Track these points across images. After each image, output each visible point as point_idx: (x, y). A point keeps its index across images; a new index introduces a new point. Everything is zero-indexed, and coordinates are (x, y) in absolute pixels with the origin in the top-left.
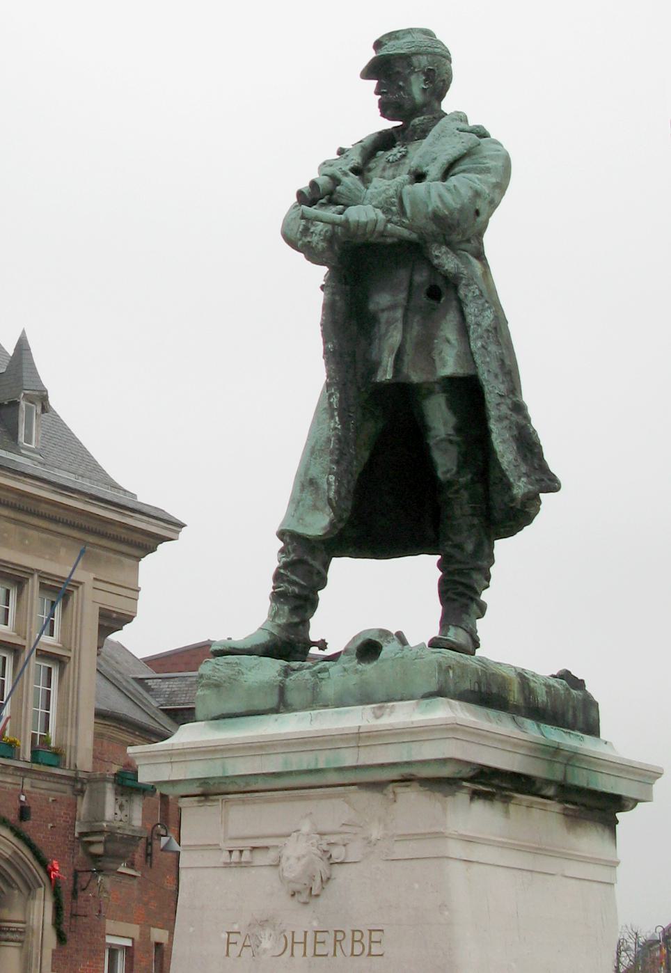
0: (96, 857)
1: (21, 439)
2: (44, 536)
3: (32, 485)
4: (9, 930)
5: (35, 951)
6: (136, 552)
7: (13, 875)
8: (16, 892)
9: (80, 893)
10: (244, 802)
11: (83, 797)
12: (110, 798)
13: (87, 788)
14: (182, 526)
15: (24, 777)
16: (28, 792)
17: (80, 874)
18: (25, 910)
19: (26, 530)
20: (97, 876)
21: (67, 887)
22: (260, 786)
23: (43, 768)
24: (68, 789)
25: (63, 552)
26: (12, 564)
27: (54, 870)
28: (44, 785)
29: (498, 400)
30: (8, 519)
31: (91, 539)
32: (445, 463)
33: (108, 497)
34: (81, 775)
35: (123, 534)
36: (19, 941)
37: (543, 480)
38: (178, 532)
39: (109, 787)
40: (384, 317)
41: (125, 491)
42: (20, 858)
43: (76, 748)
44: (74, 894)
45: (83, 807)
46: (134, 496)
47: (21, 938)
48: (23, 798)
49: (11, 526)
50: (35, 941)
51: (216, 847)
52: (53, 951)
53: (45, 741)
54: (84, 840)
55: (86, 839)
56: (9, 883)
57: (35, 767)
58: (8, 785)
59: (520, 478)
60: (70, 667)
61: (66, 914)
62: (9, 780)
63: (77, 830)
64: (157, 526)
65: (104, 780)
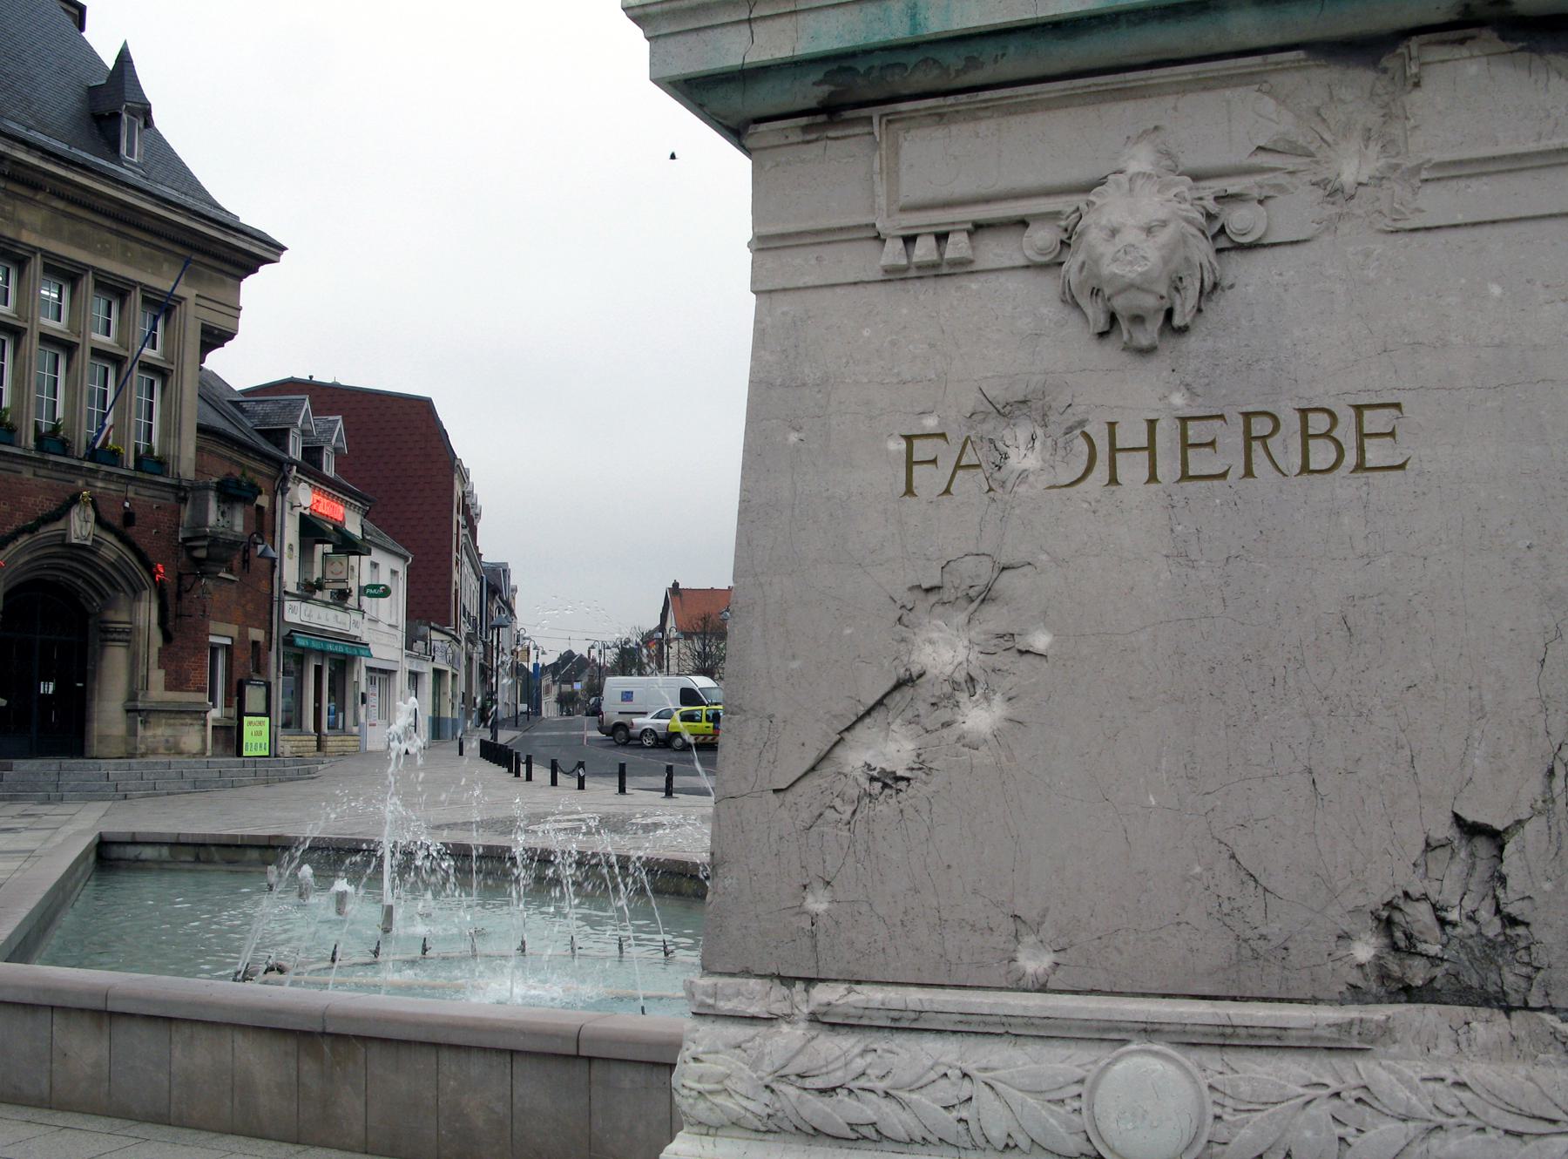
0: (198, 562)
1: (123, 151)
2: (145, 249)
3: (136, 197)
4: (116, 631)
5: (142, 650)
7: (119, 579)
8: (122, 594)
9: (184, 595)
11: (186, 504)
12: (213, 506)
13: (190, 495)
14: (283, 249)
16: (132, 499)
18: (131, 612)
19: (125, 241)
20: (200, 580)
21: (171, 589)
23: (147, 476)
24: (172, 497)
25: (166, 267)
26: (114, 275)
27: (160, 573)
30: (110, 230)
31: (195, 257)
36: (126, 641)
38: (279, 255)
42: (126, 562)
43: (179, 457)
44: (179, 596)
45: (186, 513)
47: (128, 638)
48: (127, 504)
49: (114, 238)
50: (142, 641)
52: (159, 649)
53: (150, 449)
54: (187, 546)
55: (188, 544)
56: (114, 585)
57: (139, 474)
58: (112, 492)
60: (172, 380)
61: (171, 614)
62: (113, 487)
63: (181, 536)
65: (207, 487)
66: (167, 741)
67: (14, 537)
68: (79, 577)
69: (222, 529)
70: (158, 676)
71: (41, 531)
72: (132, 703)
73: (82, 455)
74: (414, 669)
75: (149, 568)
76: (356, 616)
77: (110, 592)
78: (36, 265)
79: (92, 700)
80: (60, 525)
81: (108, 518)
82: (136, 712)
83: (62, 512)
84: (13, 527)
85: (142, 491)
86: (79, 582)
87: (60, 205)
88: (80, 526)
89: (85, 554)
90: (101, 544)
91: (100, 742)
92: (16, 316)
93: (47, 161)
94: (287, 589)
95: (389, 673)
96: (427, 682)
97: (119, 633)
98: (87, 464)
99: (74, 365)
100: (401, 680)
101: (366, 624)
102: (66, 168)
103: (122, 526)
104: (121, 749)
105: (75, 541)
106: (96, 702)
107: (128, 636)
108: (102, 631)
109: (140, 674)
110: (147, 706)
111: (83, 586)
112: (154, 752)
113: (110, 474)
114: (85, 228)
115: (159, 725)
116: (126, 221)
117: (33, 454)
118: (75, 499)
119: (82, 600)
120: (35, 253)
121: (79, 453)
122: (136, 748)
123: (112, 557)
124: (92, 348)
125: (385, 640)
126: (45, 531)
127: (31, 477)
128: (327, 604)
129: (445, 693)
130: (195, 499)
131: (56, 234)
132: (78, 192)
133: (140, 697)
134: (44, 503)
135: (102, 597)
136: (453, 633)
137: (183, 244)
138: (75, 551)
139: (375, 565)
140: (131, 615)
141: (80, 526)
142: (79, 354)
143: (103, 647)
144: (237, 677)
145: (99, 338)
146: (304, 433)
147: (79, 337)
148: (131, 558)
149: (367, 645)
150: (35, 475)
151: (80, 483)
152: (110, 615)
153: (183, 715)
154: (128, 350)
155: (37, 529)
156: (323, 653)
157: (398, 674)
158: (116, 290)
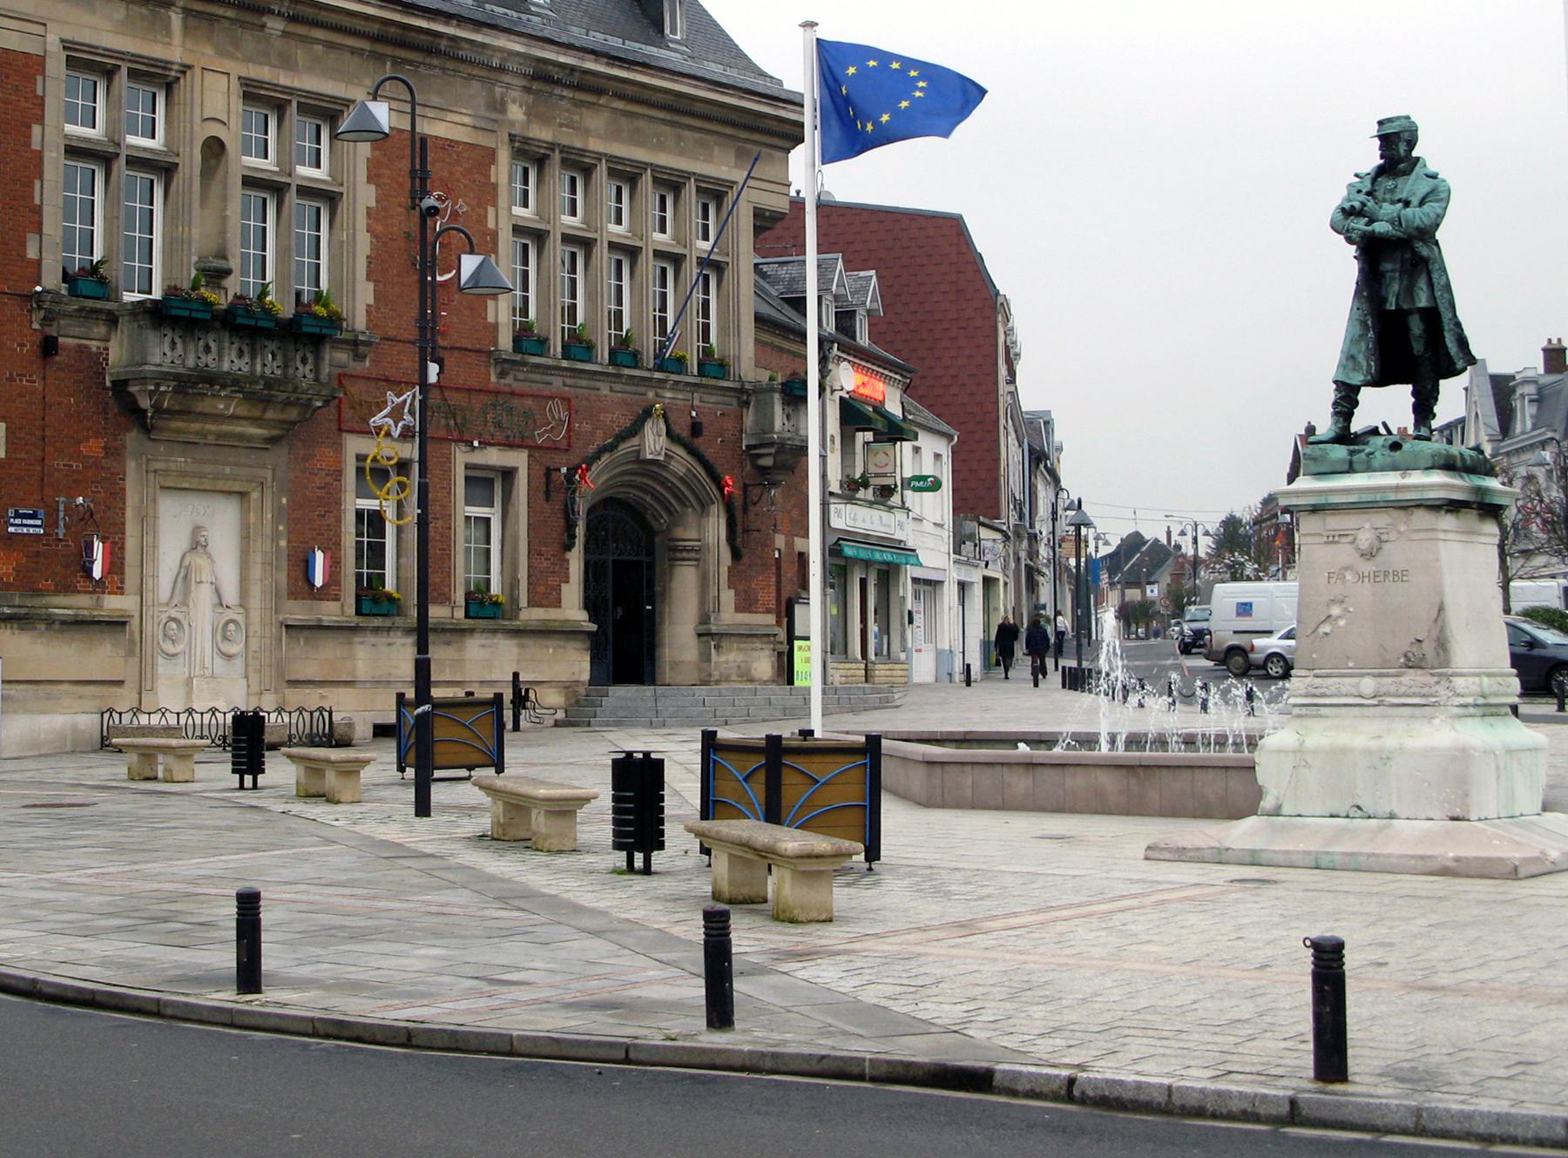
0: (763, 471)
1: (667, 31)
2: (697, 135)
4: (685, 549)
5: (712, 569)
6: (786, 144)
7: (688, 493)
9: (751, 508)
12: (778, 408)
13: (753, 399)
18: (700, 527)
21: (738, 503)
24: (735, 402)
28: (713, 399)
30: (664, 122)
31: (743, 135)
33: (760, 90)
34: (747, 386)
35: (774, 125)
36: (696, 560)
39: (777, 396)
41: (771, 77)
44: (745, 510)
45: (749, 418)
46: (780, 83)
48: (694, 414)
49: (667, 129)
50: (712, 558)
53: (707, 352)
54: (752, 453)
56: (681, 499)
57: (704, 381)
60: (728, 274)
61: (739, 529)
62: (680, 396)
63: (744, 443)
65: (772, 390)
66: (739, 667)
68: (647, 492)
69: (789, 435)
70: (728, 597)
73: (651, 365)
74: (963, 578)
76: (900, 516)
77: (678, 508)
78: (602, 170)
79: (662, 622)
80: (635, 441)
81: (676, 429)
82: (708, 636)
83: (635, 429)
85: (707, 398)
86: (648, 498)
87: (619, 105)
88: (653, 442)
90: (672, 458)
91: (672, 669)
92: (584, 226)
93: (612, 65)
94: (831, 489)
95: (934, 584)
96: (978, 590)
98: (657, 375)
99: (638, 272)
100: (950, 593)
101: (910, 525)
102: (628, 69)
103: (689, 436)
104: (694, 676)
107: (697, 554)
109: (711, 595)
110: (722, 629)
112: (727, 680)
113: (677, 383)
114: (641, 123)
115: (731, 650)
116: (680, 109)
117: (611, 370)
118: (648, 413)
119: (649, 517)
122: (710, 675)
123: (681, 471)
124: (655, 251)
125: (930, 542)
126: (625, 447)
128: (871, 504)
129: (996, 609)
130: (758, 402)
131: (615, 135)
132: (636, 89)
134: (620, 419)
135: (670, 513)
136: (1004, 528)
137: (733, 124)
138: (648, 467)
139: (917, 450)
141: (653, 442)
142: (642, 258)
143: (672, 567)
144: (785, 596)
146: (836, 298)
149: (914, 551)
151: (651, 395)
152: (679, 533)
153: (755, 640)
155: (616, 447)
156: (867, 564)
157: (946, 584)
158: (671, 184)
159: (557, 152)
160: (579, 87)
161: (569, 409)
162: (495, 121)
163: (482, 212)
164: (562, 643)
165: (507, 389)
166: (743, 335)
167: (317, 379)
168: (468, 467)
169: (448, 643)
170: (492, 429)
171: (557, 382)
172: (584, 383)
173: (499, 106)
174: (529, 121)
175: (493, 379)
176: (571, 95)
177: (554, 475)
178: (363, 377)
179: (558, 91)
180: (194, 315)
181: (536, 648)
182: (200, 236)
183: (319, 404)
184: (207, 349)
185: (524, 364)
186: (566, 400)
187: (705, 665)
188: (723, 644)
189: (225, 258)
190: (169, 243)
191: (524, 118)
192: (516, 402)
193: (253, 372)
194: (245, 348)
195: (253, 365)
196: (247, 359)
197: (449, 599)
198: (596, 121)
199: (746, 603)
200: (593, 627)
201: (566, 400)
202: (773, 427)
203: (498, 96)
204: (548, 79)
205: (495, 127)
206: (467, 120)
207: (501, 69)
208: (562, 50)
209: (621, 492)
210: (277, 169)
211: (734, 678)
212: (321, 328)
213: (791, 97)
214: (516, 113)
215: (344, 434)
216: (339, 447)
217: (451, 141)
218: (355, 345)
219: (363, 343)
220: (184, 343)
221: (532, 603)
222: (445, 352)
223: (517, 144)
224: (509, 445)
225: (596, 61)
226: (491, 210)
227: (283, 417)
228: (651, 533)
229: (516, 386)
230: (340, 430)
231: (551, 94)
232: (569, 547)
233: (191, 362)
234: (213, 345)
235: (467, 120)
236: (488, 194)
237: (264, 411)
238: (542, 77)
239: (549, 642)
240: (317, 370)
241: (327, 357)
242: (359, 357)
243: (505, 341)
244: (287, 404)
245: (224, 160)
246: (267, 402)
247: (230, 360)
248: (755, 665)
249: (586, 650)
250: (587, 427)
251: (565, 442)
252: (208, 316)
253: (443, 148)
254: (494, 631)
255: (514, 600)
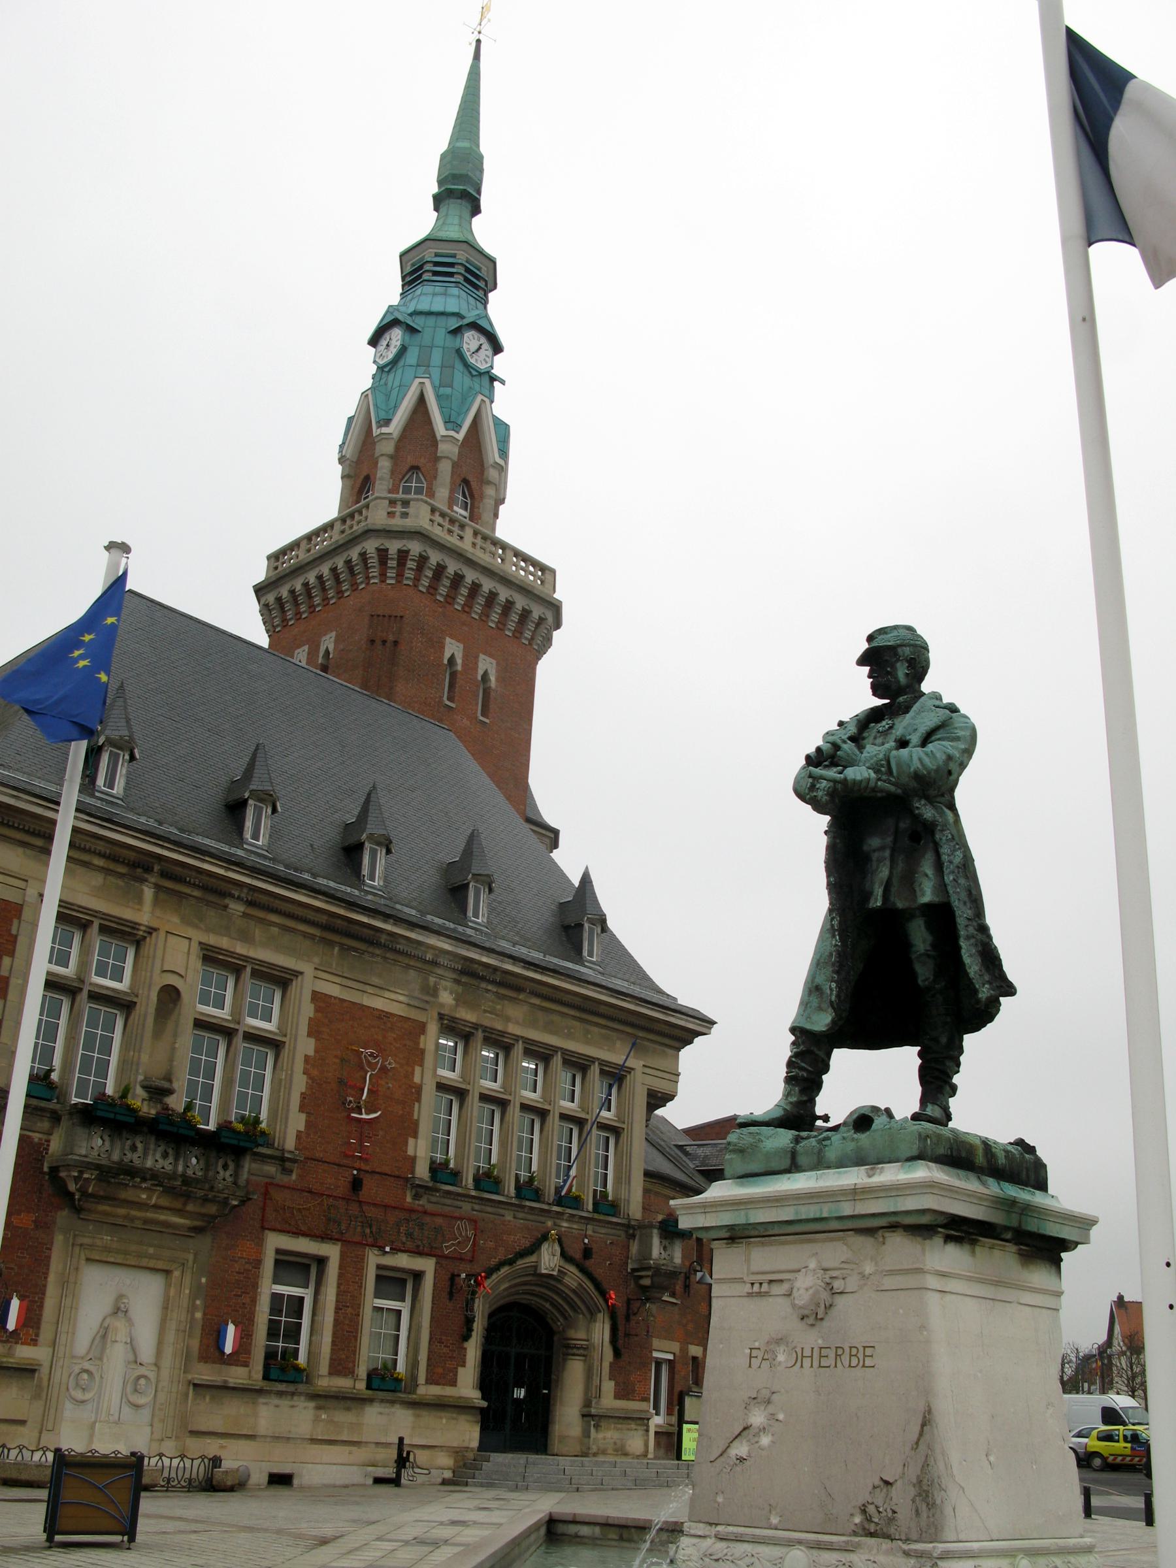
0: (645, 1289)
1: (585, 953)
2: (603, 1031)
4: (575, 1347)
5: (596, 1363)
6: (677, 1044)
7: (579, 1303)
8: (581, 1316)
9: (632, 1317)
10: (763, 1244)
11: (634, 1240)
12: (656, 1241)
13: (638, 1233)
14: (713, 1023)
15: (587, 1224)
16: (590, 1236)
17: (632, 1302)
18: (588, 1331)
19: (588, 1027)
22: (776, 1231)
23: (602, 1217)
24: (623, 1234)
25: (618, 1044)
26: (578, 1053)
27: (612, 1298)
28: (603, 1231)
29: (967, 923)
30: (574, 1017)
31: (641, 1034)
32: (924, 973)
34: (633, 1223)
35: (667, 1030)
36: (584, 1356)
37: (1002, 986)
38: (710, 1028)
39: (655, 1231)
40: (875, 856)
41: (668, 995)
42: (584, 1289)
43: (628, 1201)
44: (628, 1318)
45: (634, 1248)
46: (675, 999)
47: (585, 1353)
48: (586, 1241)
49: (577, 1024)
50: (596, 1356)
51: (740, 1280)
52: (611, 1363)
53: (604, 1195)
55: (636, 1274)
57: (596, 1216)
58: (574, 1231)
59: (984, 985)
60: (624, 1136)
61: (621, 1334)
63: (630, 1267)
64: (694, 1023)
65: (651, 1226)
66: (615, 1443)
67: (497, 1268)
68: (547, 1300)
69: (664, 1262)
70: (609, 1386)
71: (518, 1263)
72: (586, 1410)
73: (551, 1201)
75: (603, 1294)
77: (571, 1314)
78: (519, 1048)
80: (533, 1258)
82: (588, 1416)
83: (534, 1248)
84: (497, 1260)
86: (548, 1305)
87: (536, 1001)
89: (553, 1282)
90: (566, 1274)
92: (502, 1090)
93: (528, 969)
97: (578, 1348)
98: (555, 1208)
99: (546, 1129)
102: (542, 973)
103: (582, 1258)
104: (577, 1449)
105: (544, 1271)
106: (558, 1407)
107: (585, 1351)
108: (566, 1347)
109: (594, 1384)
110: (601, 1412)
111: (550, 1308)
112: (604, 1452)
113: (573, 1216)
114: (556, 1018)
116: (587, 1010)
117: (514, 1201)
118: (545, 1237)
119: (550, 1321)
120: (518, 1041)
121: (549, 1199)
122: (589, 1448)
126: (522, 1263)
127: (512, 1219)
131: (533, 1024)
133: (593, 1405)
135: (565, 1318)
137: (632, 1025)
138: (545, 1280)
140: (588, 1335)
141: (549, 1259)
142: (550, 1119)
143: (565, 1360)
144: (677, 1389)
145: (567, 1105)
147: (550, 1104)
148: (589, 1285)
150: (515, 1217)
151: (550, 1223)
152: (572, 1333)
153: (630, 1422)
154: (588, 1113)
155: (515, 1262)
158: (579, 1065)
159: (480, 1031)
160: (501, 984)
161: (475, 1229)
162: (427, 1002)
163: (410, 1069)
164: (454, 1415)
165: (420, 1208)
166: (633, 1183)
167: (235, 1183)
168: (379, 1267)
169: (348, 1409)
170: (404, 1239)
171: (466, 1207)
172: (489, 1209)
173: (434, 992)
174: (457, 1005)
175: (409, 1199)
176: (495, 990)
177: (457, 1278)
178: (288, 1188)
179: (483, 985)
180: (119, 1117)
181: (429, 1418)
182: (149, 1062)
183: (235, 1203)
184: (134, 1148)
185: (438, 1190)
186: (474, 1222)
187: (586, 1440)
188: (602, 1424)
189: (170, 1081)
190: (123, 1063)
191: (454, 1002)
192: (427, 1219)
193: (175, 1172)
194: (170, 1151)
195: (176, 1165)
196: (171, 1159)
197: (354, 1372)
198: (516, 1012)
199: (623, 1393)
200: (484, 1404)
201: (474, 1222)
202: (650, 1254)
203: (432, 984)
204: (473, 975)
205: (427, 1007)
206: (401, 998)
207: (434, 963)
208: (485, 953)
209: (525, 1299)
210: (230, 1018)
211: (610, 1451)
212: (239, 1140)
213: (678, 1008)
214: (446, 998)
215: (267, 1231)
216: (260, 1242)
217: (387, 1013)
218: (282, 1160)
219: (289, 1160)
220: (112, 1142)
221: (429, 1381)
222: (367, 1175)
223: (446, 1022)
224: (418, 1252)
225: (514, 964)
226: (418, 1069)
227: (204, 1211)
228: (551, 1332)
229: (430, 1207)
230: (263, 1228)
231: (478, 987)
232: (466, 1337)
233: (116, 1157)
234: (140, 1146)
235: (401, 998)
236: (418, 1056)
237: (185, 1204)
238: (469, 973)
239: (443, 1414)
240: (236, 1175)
241: (247, 1166)
242: (287, 1171)
243: (422, 1171)
244: (205, 1200)
245: (178, 1006)
246: (188, 1197)
247: (155, 1159)
248: (629, 1442)
249: (477, 1422)
250: (491, 1244)
251: (470, 1255)
252: (132, 1120)
253: (379, 1018)
254: (393, 1402)
255: (414, 1378)
